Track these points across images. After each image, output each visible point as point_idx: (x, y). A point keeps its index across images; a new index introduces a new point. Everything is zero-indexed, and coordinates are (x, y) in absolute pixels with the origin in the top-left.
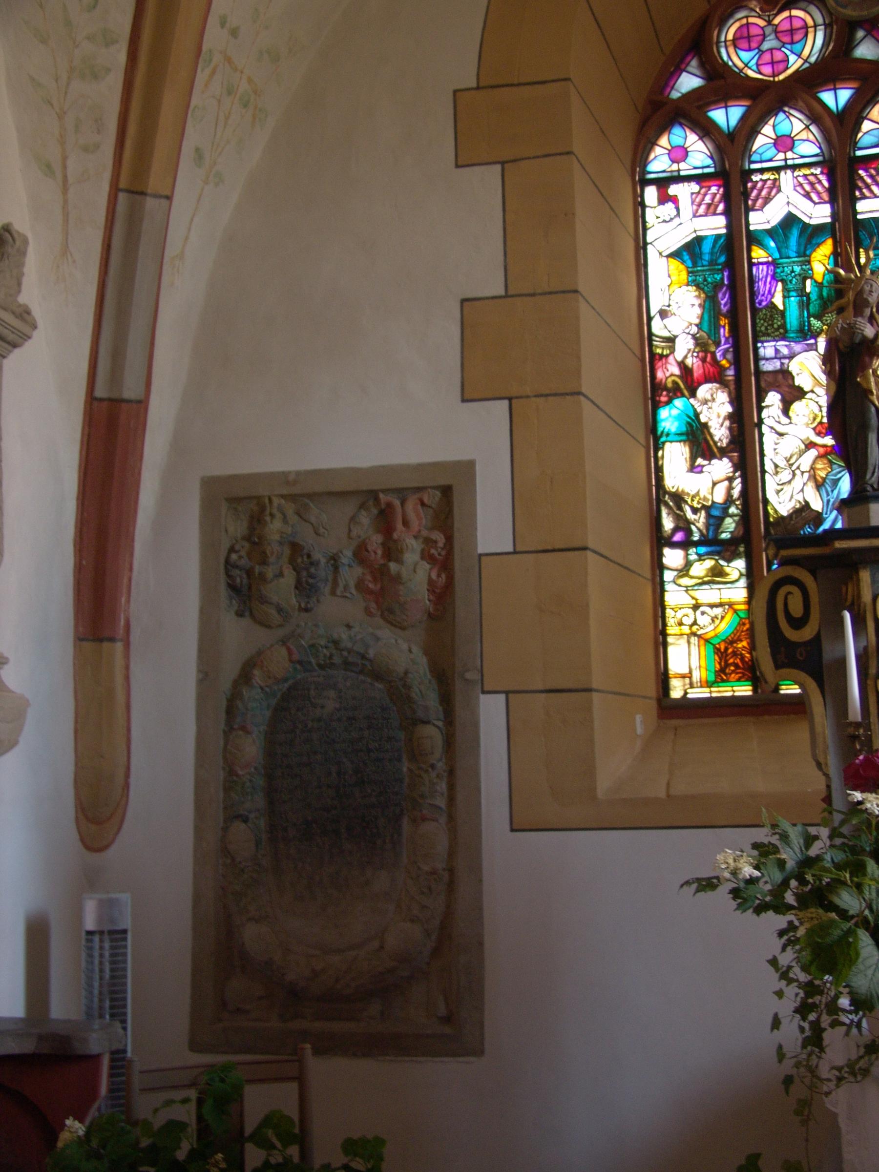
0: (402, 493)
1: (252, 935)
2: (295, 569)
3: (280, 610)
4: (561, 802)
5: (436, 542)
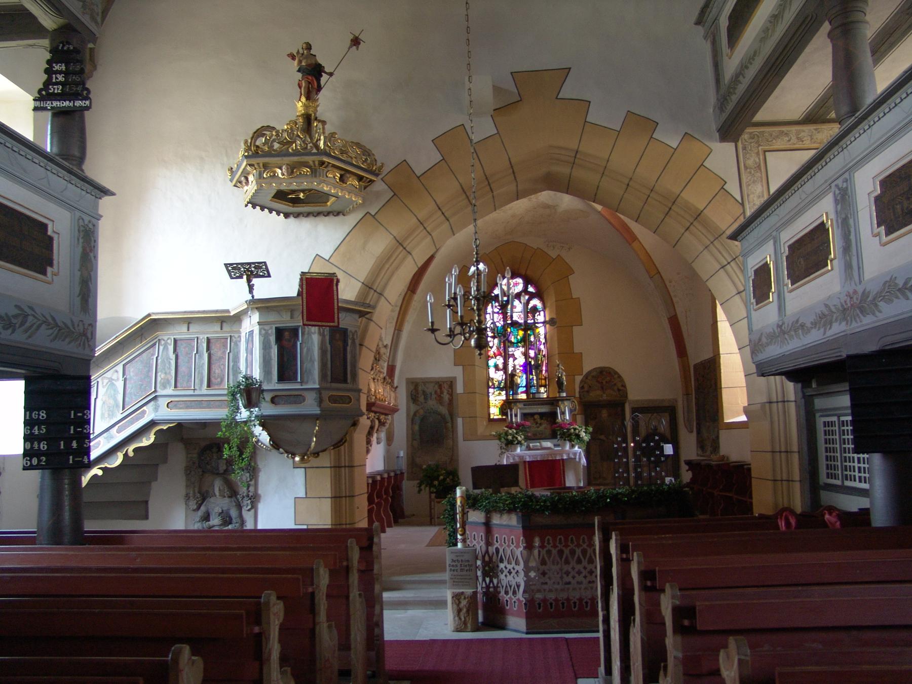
4: (472, 435)
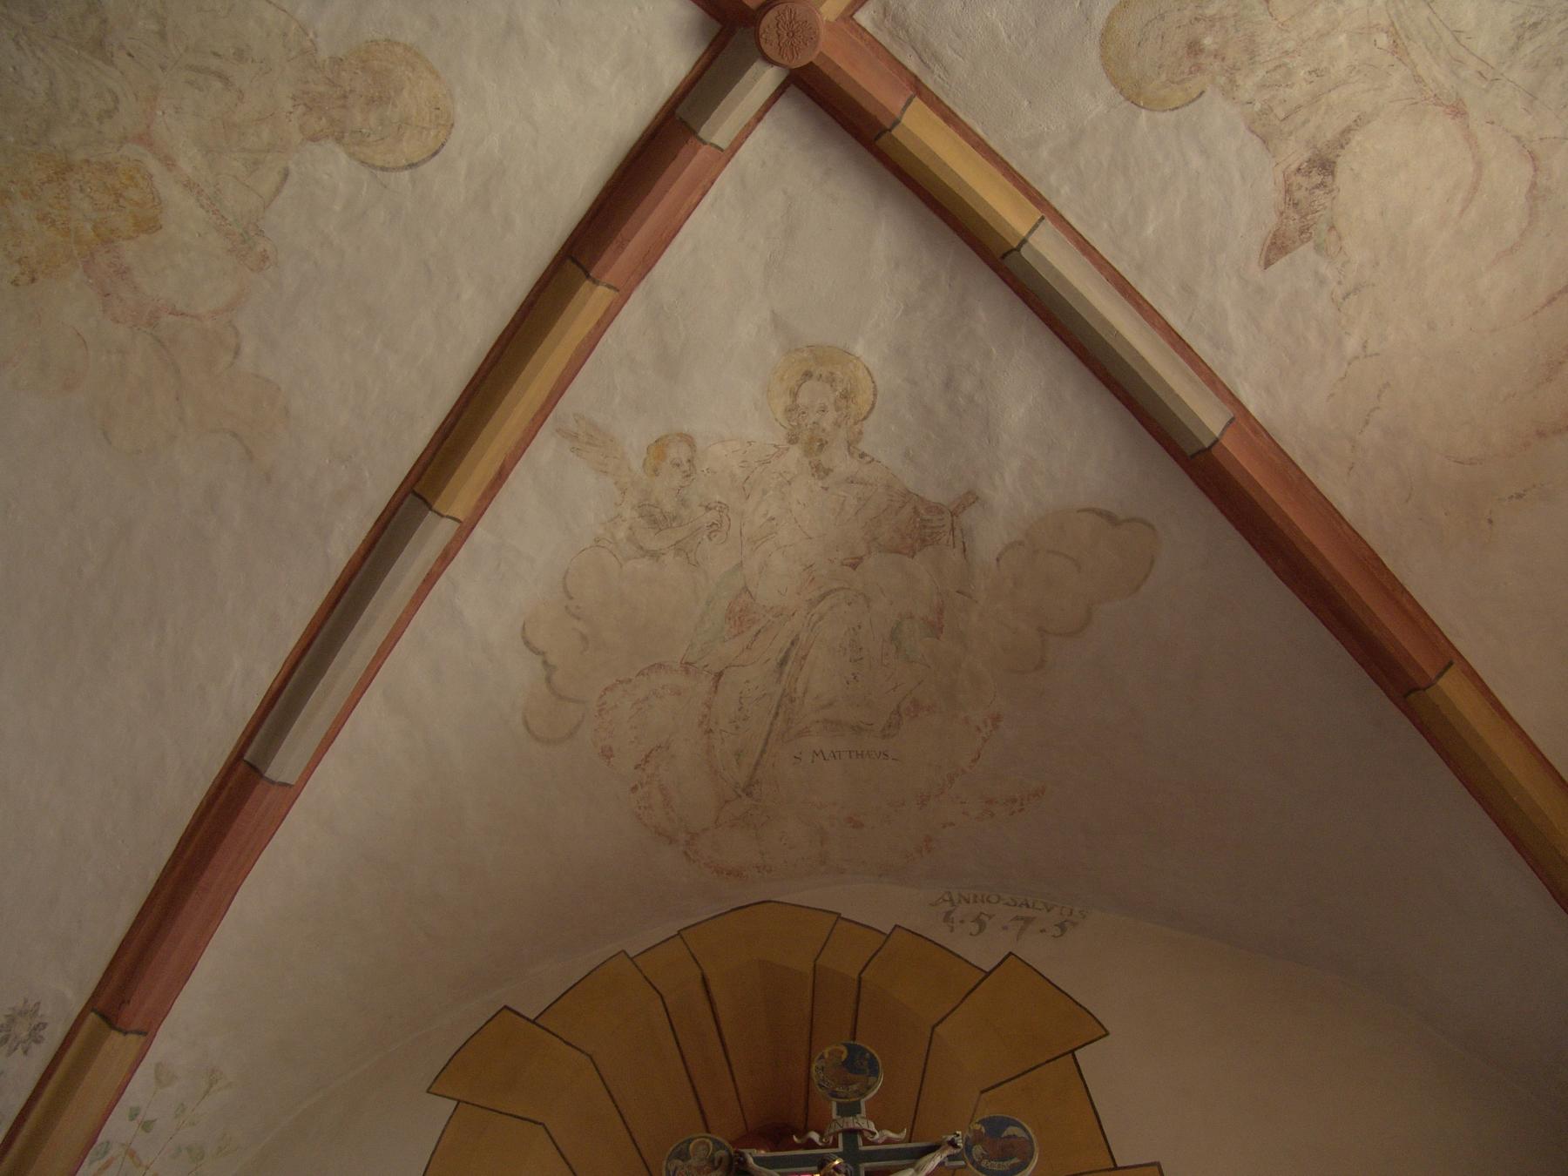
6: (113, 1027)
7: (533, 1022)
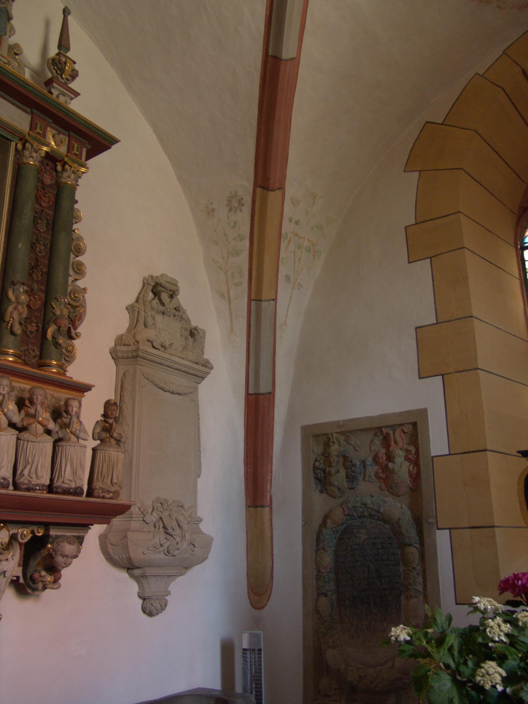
0: (393, 427)
1: (330, 654)
2: (345, 469)
3: (339, 489)
5: (411, 451)
6: (269, 190)
7: (442, 124)
